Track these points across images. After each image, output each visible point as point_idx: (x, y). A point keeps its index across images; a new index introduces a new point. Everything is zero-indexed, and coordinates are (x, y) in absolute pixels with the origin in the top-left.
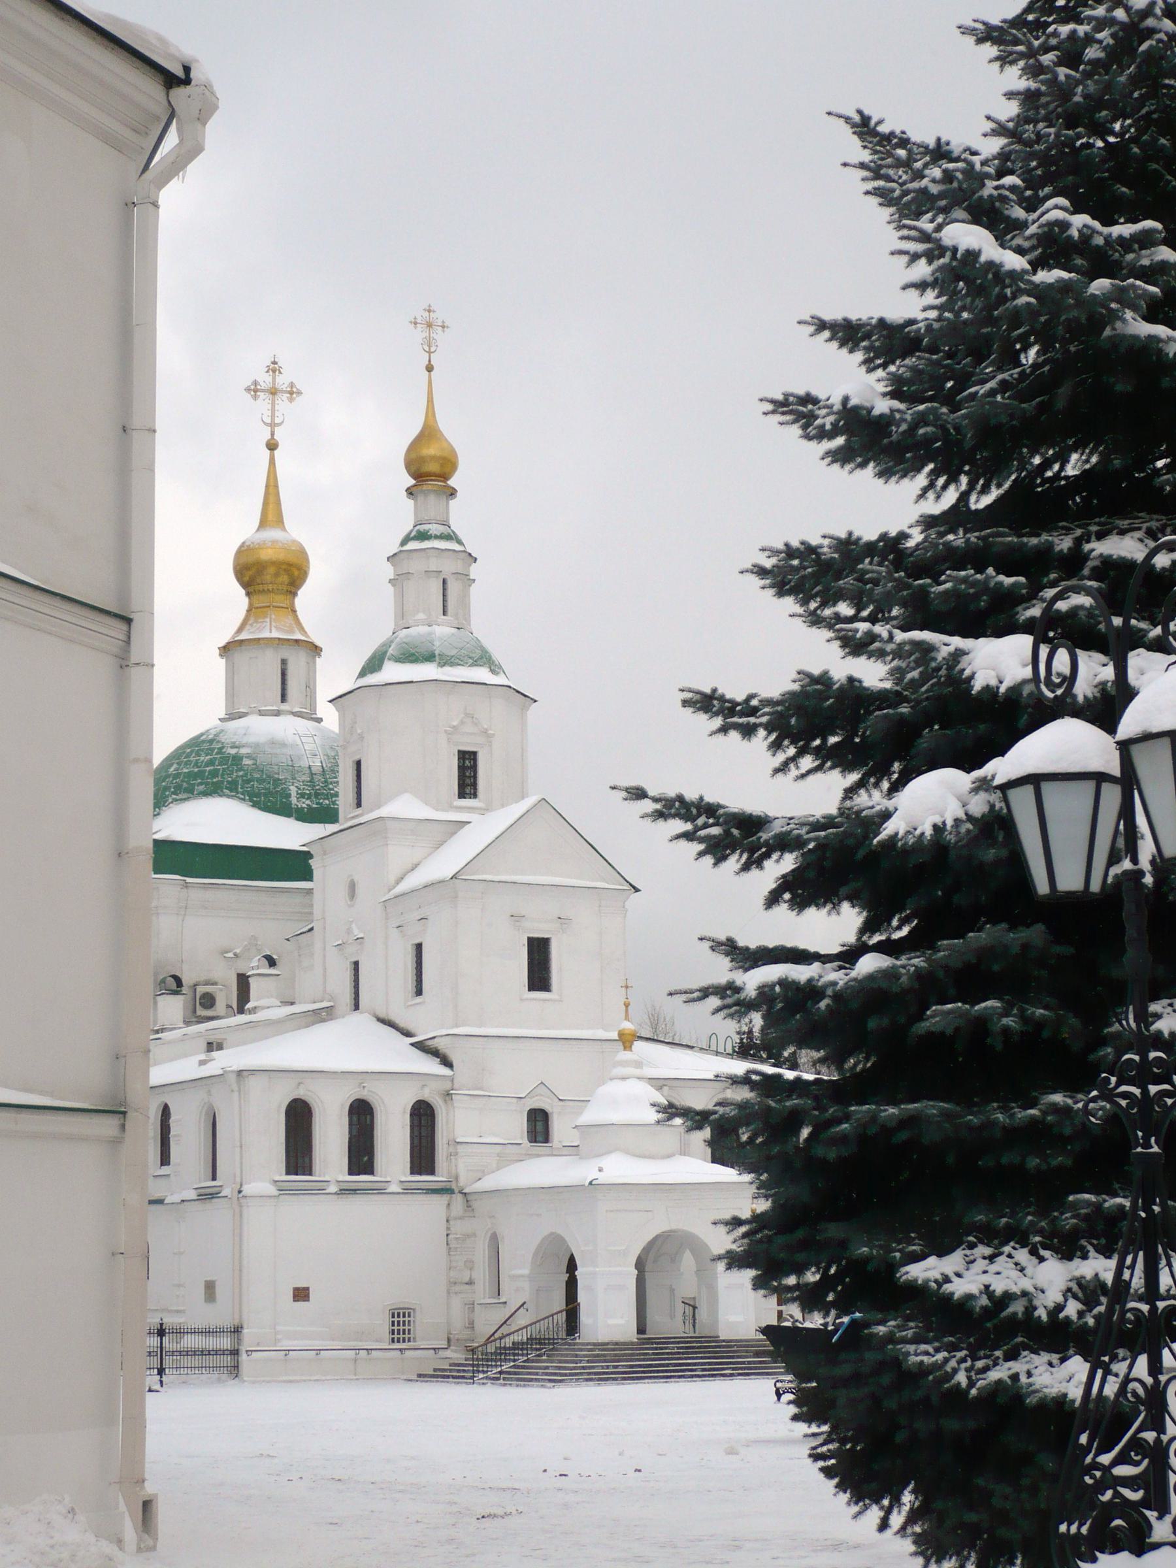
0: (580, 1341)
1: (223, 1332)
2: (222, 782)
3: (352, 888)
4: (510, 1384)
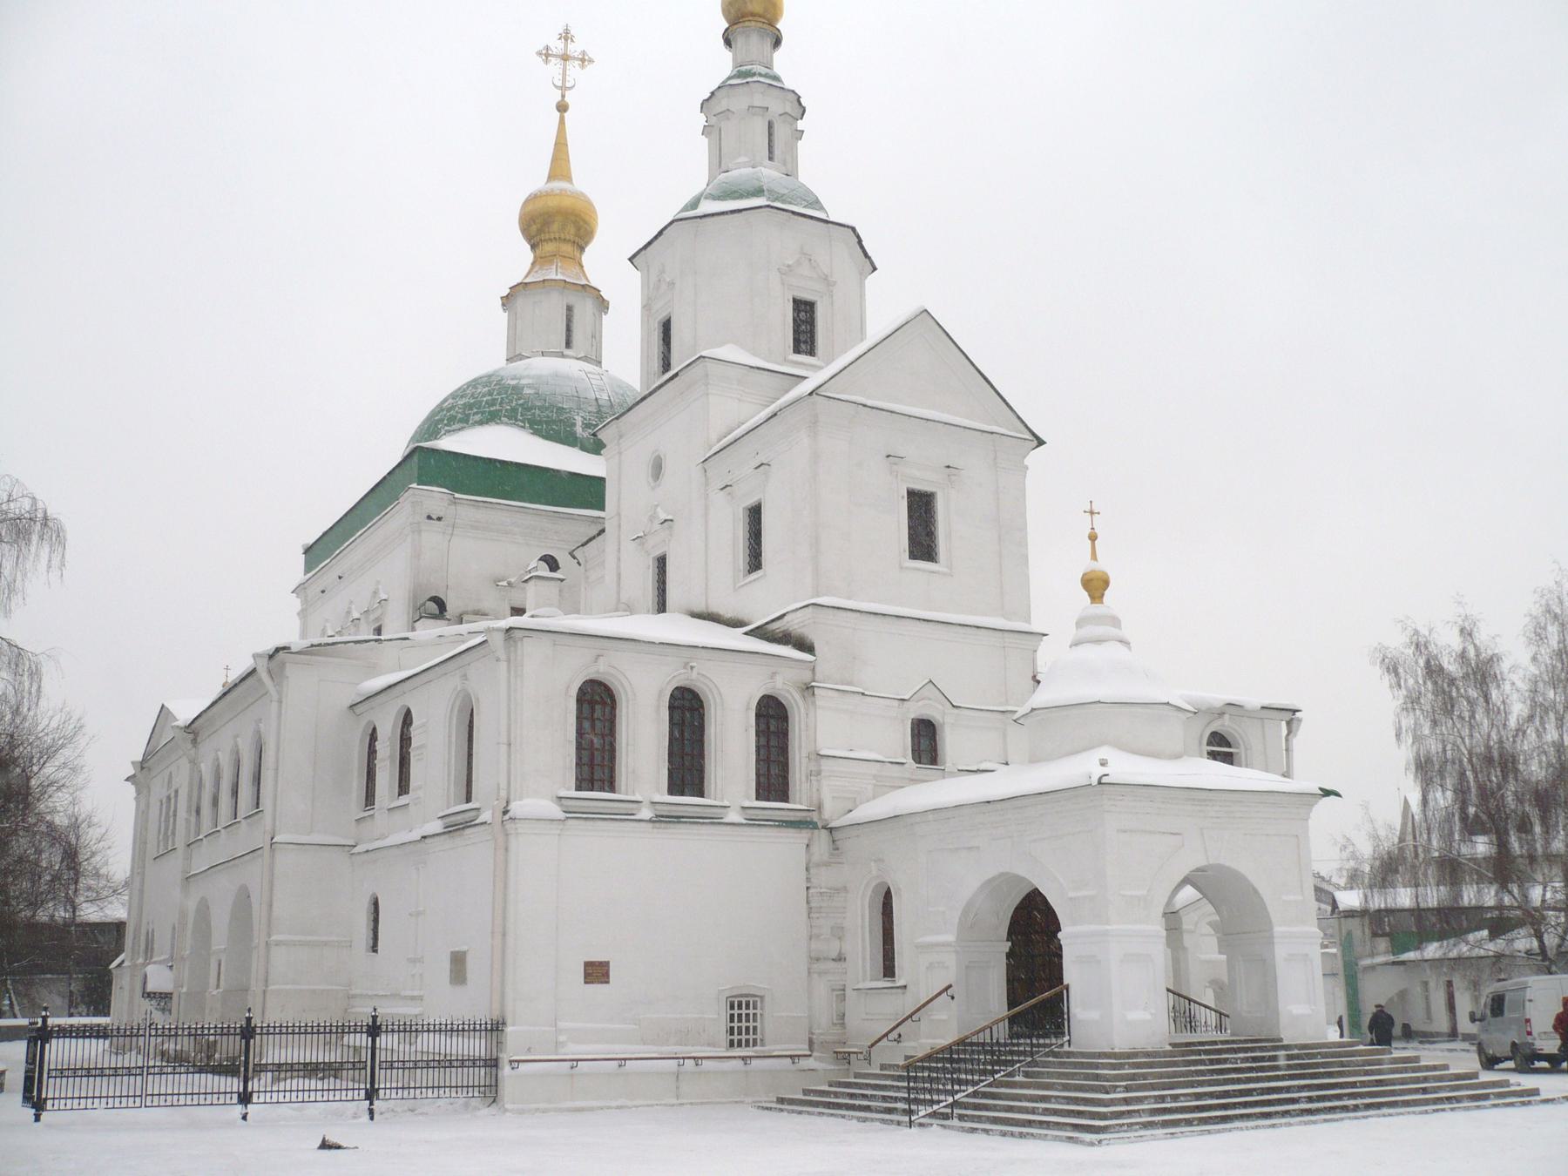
0: (1071, 1049)
1: (474, 1030)
2: (501, 411)
3: (657, 468)
4: (986, 1131)
